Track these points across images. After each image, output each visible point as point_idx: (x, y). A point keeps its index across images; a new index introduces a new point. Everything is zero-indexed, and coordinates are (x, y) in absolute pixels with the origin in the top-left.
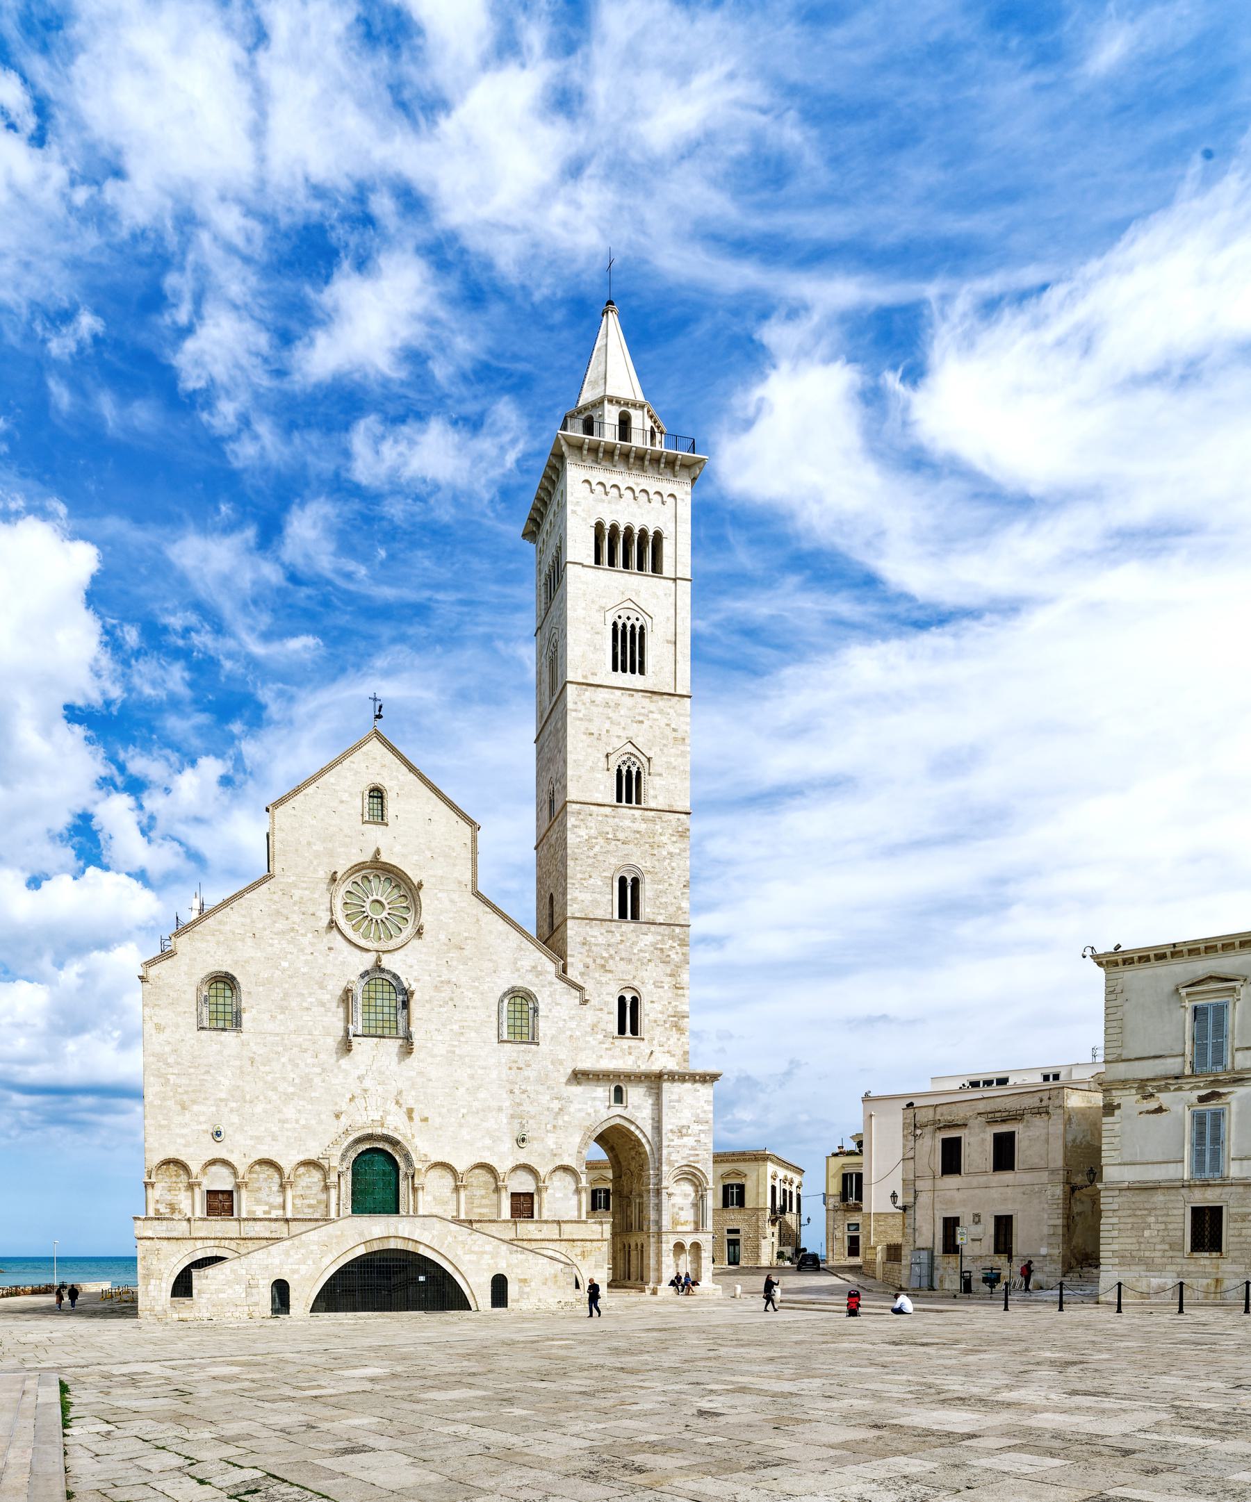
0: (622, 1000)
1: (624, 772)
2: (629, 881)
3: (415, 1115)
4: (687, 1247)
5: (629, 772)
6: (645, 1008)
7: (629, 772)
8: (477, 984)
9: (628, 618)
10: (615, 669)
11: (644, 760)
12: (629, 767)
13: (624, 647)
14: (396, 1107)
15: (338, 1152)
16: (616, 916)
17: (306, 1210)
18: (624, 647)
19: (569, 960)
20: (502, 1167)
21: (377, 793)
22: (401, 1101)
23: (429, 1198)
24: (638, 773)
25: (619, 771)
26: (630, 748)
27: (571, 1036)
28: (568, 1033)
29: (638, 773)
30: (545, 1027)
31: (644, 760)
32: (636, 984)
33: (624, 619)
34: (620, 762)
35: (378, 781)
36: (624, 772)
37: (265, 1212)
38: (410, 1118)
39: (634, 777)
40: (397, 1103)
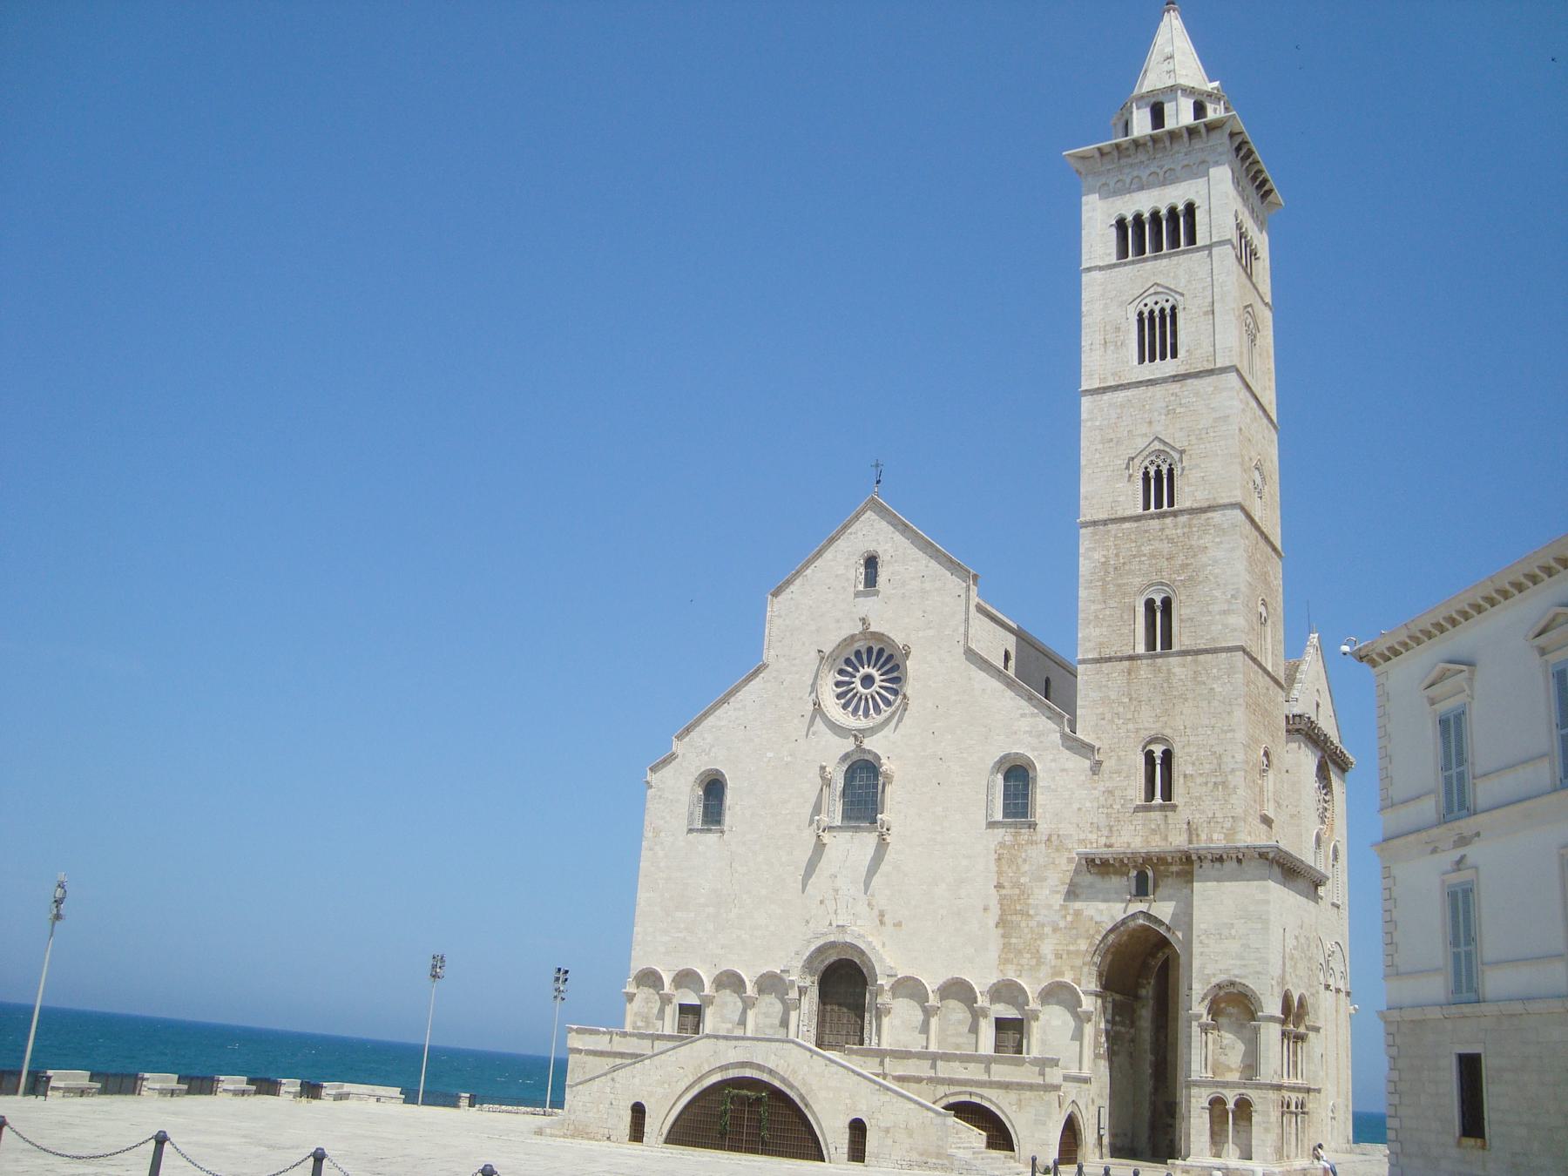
0: (1149, 757)
1: (1152, 473)
2: (1158, 603)
3: (887, 919)
4: (1231, 1105)
5: (1158, 473)
6: (1180, 766)
7: (1158, 473)
8: (965, 755)
9: (1156, 303)
10: (1141, 360)
11: (1176, 456)
12: (1158, 466)
13: (1153, 336)
14: (868, 909)
15: (798, 964)
16: (1141, 649)
17: (767, 1031)
18: (1153, 336)
19: (1079, 712)
20: (981, 984)
21: (871, 563)
22: (874, 903)
23: (897, 1022)
24: (1171, 471)
25: (1146, 474)
26: (1157, 445)
27: (1079, 809)
28: (1076, 806)
29: (1171, 471)
30: (1043, 800)
31: (1176, 456)
32: (1168, 732)
33: (1151, 304)
34: (1146, 463)
35: (872, 547)
36: (1152, 473)
37: (728, 1030)
38: (882, 923)
39: (1165, 476)
40: (869, 905)
